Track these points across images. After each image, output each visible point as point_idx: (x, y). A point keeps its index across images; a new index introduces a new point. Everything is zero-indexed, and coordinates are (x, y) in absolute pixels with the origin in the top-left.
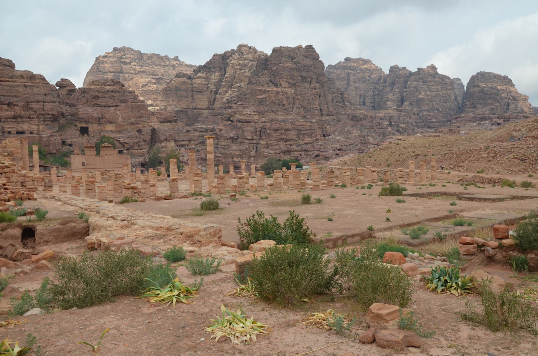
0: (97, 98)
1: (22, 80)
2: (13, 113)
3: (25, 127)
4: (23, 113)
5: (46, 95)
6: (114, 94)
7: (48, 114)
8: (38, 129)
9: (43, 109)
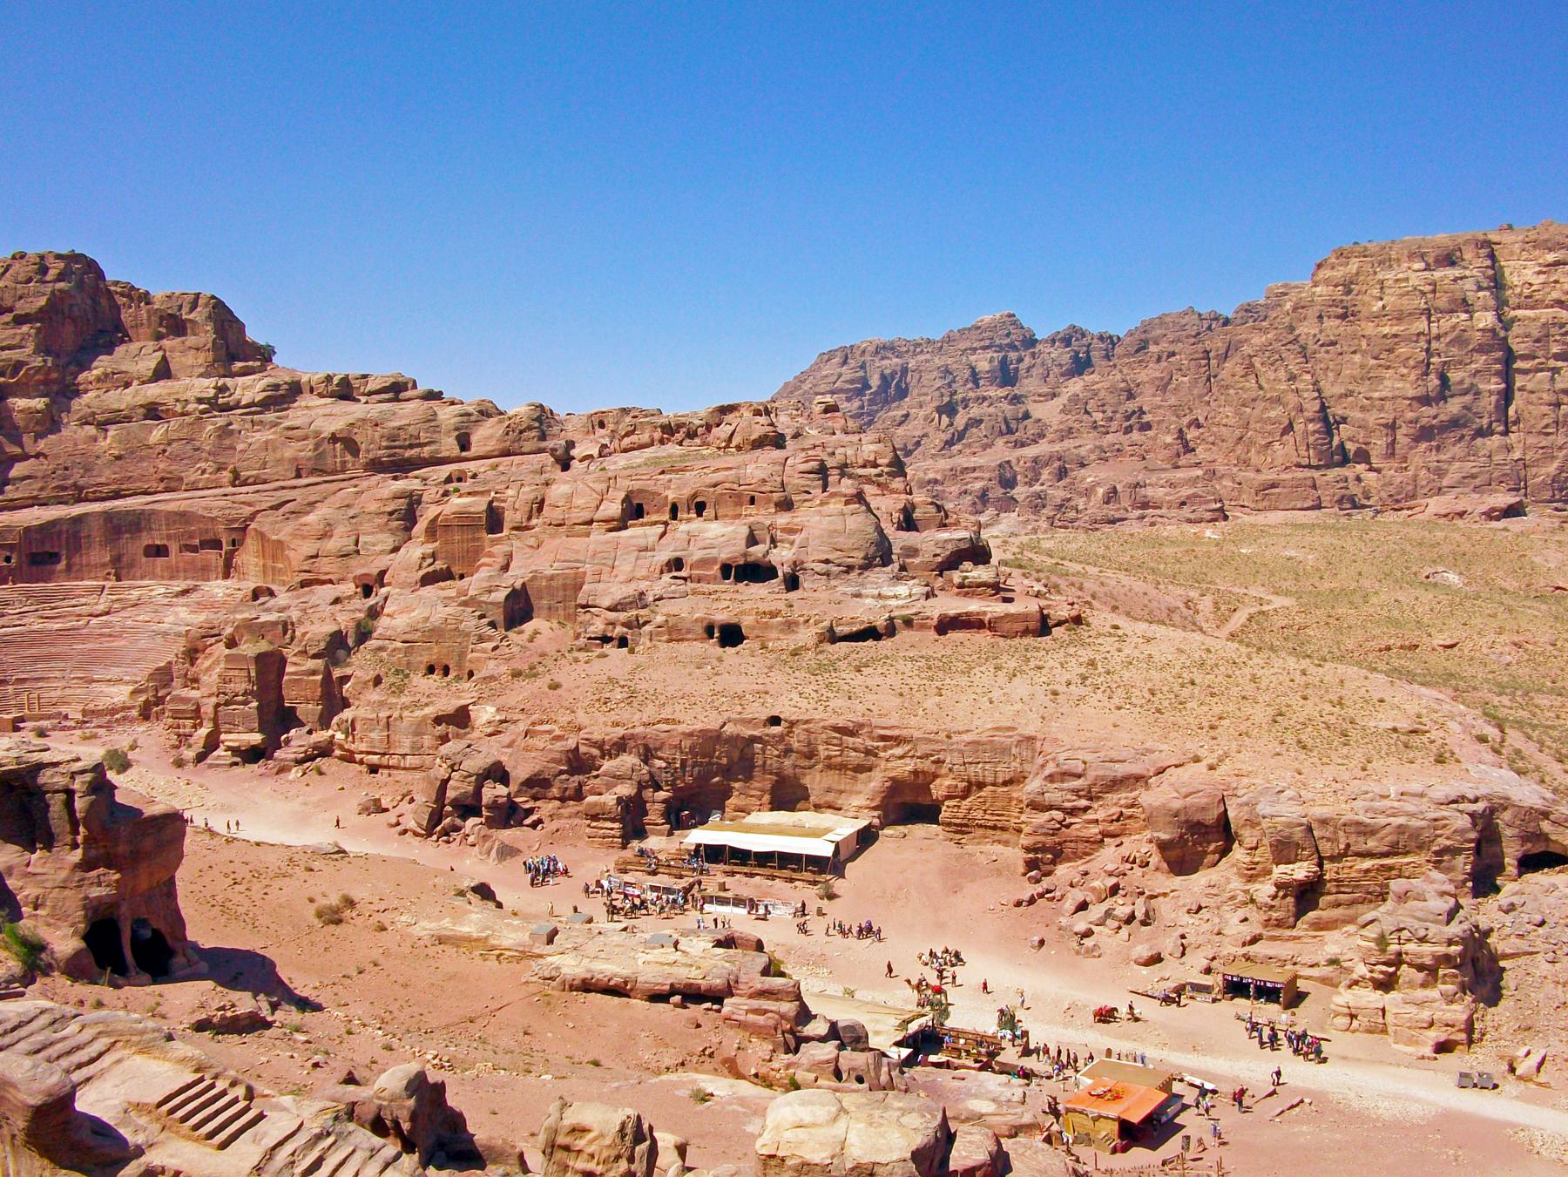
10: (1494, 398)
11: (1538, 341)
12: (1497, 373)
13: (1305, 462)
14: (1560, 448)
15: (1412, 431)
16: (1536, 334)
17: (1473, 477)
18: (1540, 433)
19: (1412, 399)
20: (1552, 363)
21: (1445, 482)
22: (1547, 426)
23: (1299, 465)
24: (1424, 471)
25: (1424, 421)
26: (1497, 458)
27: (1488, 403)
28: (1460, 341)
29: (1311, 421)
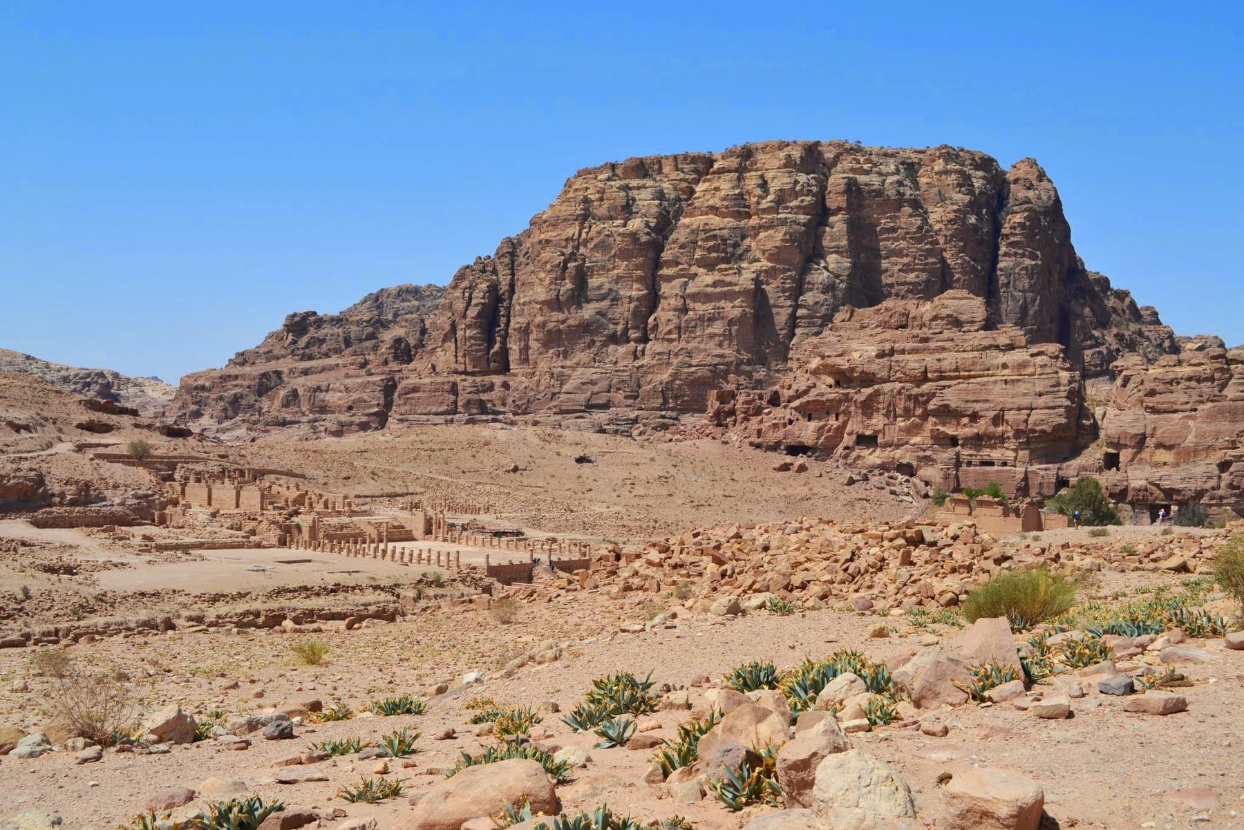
0: (1152, 393)
1: (1006, 372)
2: (976, 431)
3: (996, 454)
4: (992, 429)
5: (1040, 395)
6: (1193, 384)
7: (1034, 431)
8: (1016, 458)
9: (1026, 421)
10: (632, 306)
11: (682, 246)
12: (639, 280)
13: (461, 368)
14: (676, 355)
15: (541, 335)
16: (682, 240)
17: (593, 383)
18: (663, 339)
19: (543, 303)
20: (694, 269)
21: (565, 388)
22: (670, 332)
23: (456, 372)
24: (547, 376)
25: (551, 326)
26: (620, 366)
27: (624, 311)
28: (603, 246)
29: (469, 326)
